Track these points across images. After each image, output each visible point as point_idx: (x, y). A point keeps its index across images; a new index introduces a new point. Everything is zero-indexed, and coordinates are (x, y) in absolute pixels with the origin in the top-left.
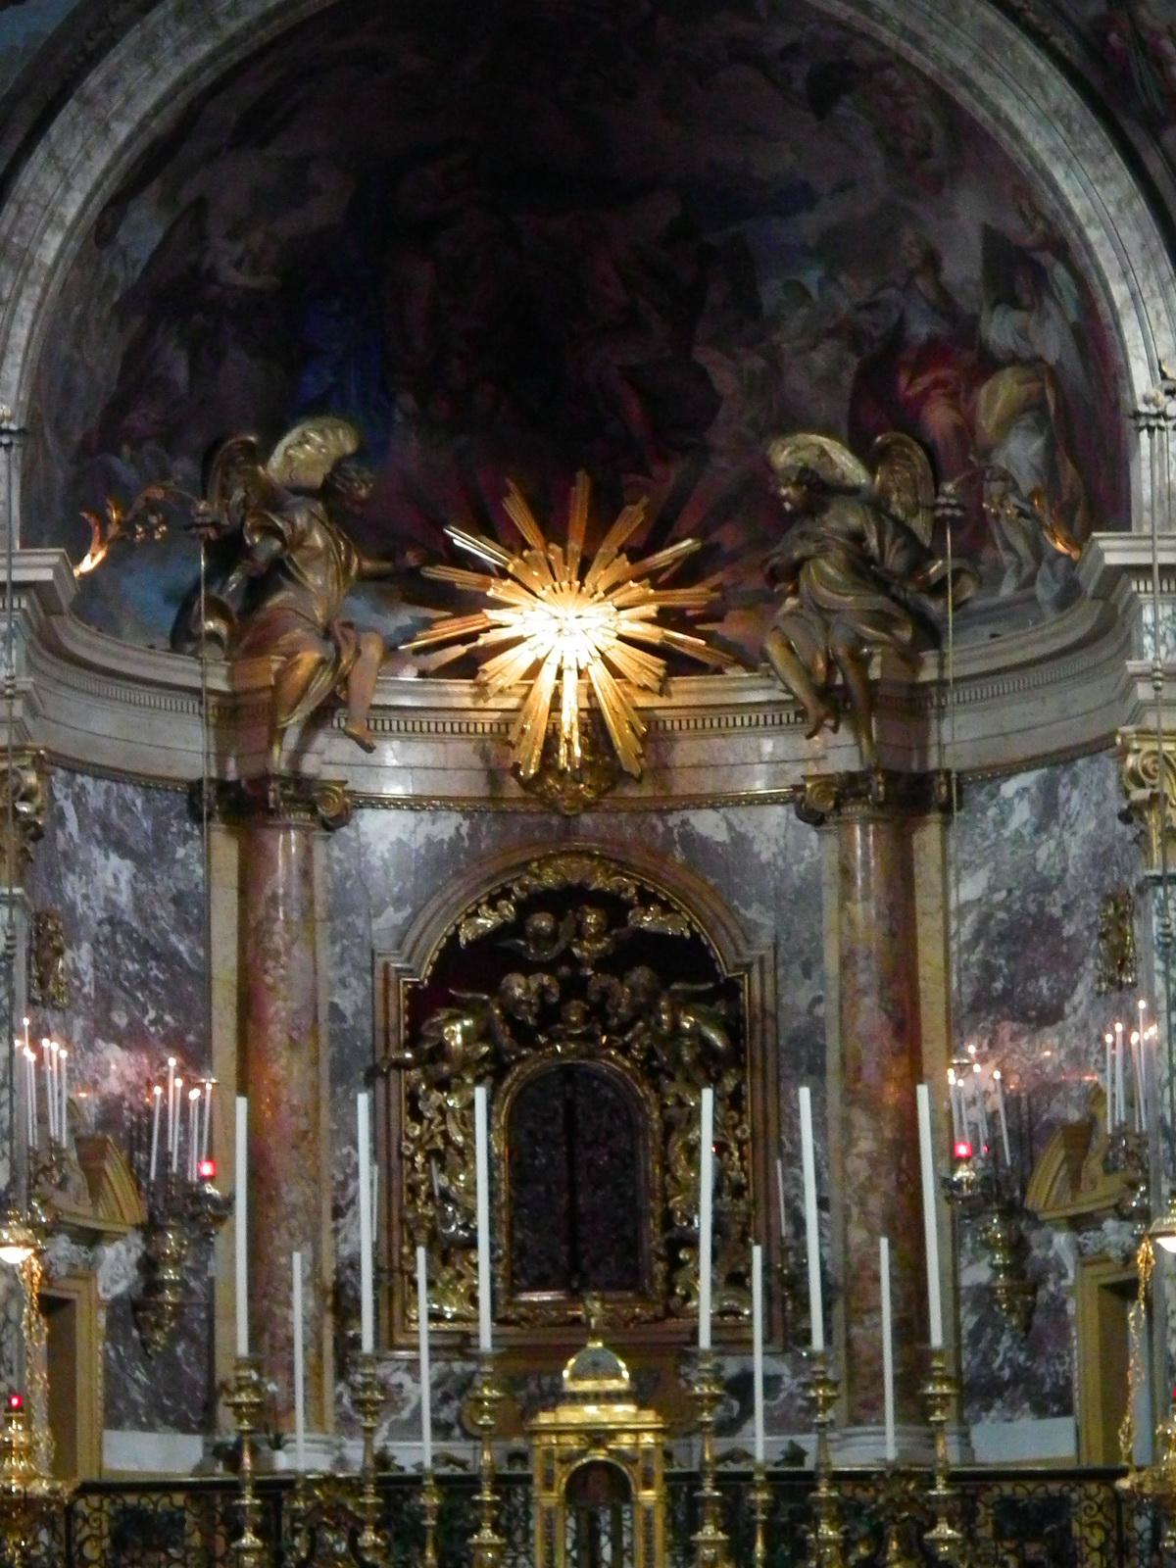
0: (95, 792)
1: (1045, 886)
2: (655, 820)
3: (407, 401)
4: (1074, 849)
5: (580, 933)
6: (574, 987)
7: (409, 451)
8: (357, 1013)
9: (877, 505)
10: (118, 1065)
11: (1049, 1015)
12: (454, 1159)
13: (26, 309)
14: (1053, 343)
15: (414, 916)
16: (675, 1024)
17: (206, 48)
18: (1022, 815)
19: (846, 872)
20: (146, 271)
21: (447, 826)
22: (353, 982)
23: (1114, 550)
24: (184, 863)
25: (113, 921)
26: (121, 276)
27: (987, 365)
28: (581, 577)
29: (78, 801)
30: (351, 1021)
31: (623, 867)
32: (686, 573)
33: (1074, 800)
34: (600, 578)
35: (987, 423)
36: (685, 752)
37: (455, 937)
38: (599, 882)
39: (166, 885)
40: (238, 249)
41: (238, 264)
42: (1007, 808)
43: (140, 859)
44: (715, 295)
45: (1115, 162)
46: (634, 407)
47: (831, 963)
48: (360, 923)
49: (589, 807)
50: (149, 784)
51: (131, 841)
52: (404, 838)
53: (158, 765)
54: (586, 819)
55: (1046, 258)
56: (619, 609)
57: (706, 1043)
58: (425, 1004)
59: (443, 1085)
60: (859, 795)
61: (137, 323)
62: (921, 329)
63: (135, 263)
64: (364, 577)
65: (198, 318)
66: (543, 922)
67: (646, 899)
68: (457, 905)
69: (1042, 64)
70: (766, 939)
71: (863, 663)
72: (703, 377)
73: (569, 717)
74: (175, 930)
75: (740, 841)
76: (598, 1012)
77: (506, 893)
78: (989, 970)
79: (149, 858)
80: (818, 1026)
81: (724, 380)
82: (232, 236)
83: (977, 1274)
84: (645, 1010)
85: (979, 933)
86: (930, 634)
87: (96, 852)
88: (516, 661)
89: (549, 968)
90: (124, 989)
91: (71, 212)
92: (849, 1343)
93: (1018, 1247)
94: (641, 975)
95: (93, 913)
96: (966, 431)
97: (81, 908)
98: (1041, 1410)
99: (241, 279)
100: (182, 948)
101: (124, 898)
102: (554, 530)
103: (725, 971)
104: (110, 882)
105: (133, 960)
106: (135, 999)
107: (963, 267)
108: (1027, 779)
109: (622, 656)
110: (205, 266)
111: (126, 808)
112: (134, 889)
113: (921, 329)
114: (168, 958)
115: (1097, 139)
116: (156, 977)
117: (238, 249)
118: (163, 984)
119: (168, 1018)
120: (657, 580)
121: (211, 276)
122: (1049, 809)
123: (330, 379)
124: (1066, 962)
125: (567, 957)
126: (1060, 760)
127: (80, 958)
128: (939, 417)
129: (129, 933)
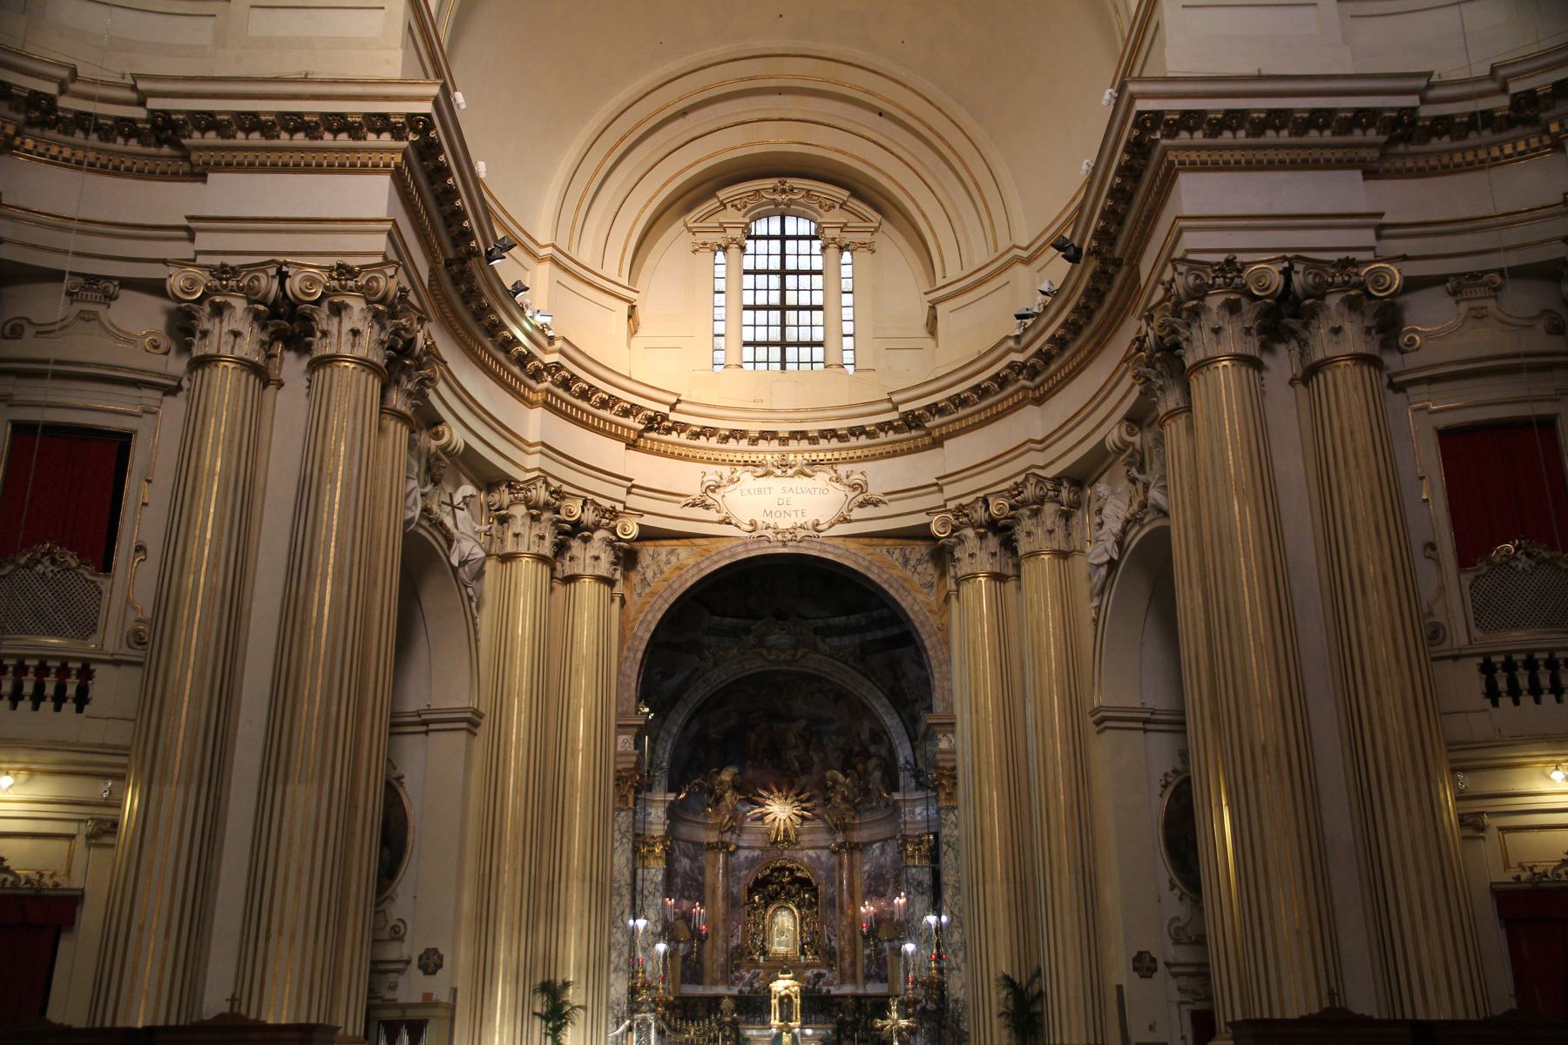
0: (682, 845)
1: (882, 867)
3: (750, 762)
4: (888, 859)
5: (784, 876)
6: (783, 888)
7: (750, 773)
9: (846, 786)
10: (685, 904)
11: (883, 895)
13: (670, 743)
14: (884, 752)
17: (708, 689)
18: (877, 852)
19: (841, 865)
21: (757, 853)
23: (897, 796)
25: (685, 872)
27: (870, 756)
29: (679, 846)
31: (794, 862)
32: (808, 800)
33: (888, 849)
34: (789, 801)
35: (870, 769)
36: (805, 838)
37: (757, 878)
38: (789, 865)
39: (697, 864)
42: (874, 850)
44: (814, 740)
45: (896, 715)
46: (797, 764)
47: (837, 883)
50: (694, 843)
55: (881, 734)
58: (751, 892)
59: (755, 909)
62: (857, 749)
64: (740, 799)
66: (776, 874)
67: (799, 869)
69: (881, 694)
72: (811, 758)
73: (782, 828)
75: (818, 857)
76: (788, 894)
78: (870, 885)
79: (694, 859)
80: (834, 897)
81: (815, 759)
83: (867, 952)
84: (798, 893)
85: (868, 877)
86: (858, 812)
88: (771, 817)
89: (777, 884)
91: (680, 722)
92: (841, 968)
93: (875, 945)
94: (797, 886)
95: (681, 871)
96: (866, 770)
98: (881, 982)
101: (688, 867)
102: (780, 791)
103: (814, 884)
107: (865, 736)
108: (878, 844)
109: (793, 817)
111: (689, 849)
113: (857, 749)
114: (697, 881)
115: (892, 710)
120: (801, 801)
122: (883, 851)
124: (887, 884)
125: (781, 881)
126: (885, 840)
127: (678, 881)
128: (860, 767)
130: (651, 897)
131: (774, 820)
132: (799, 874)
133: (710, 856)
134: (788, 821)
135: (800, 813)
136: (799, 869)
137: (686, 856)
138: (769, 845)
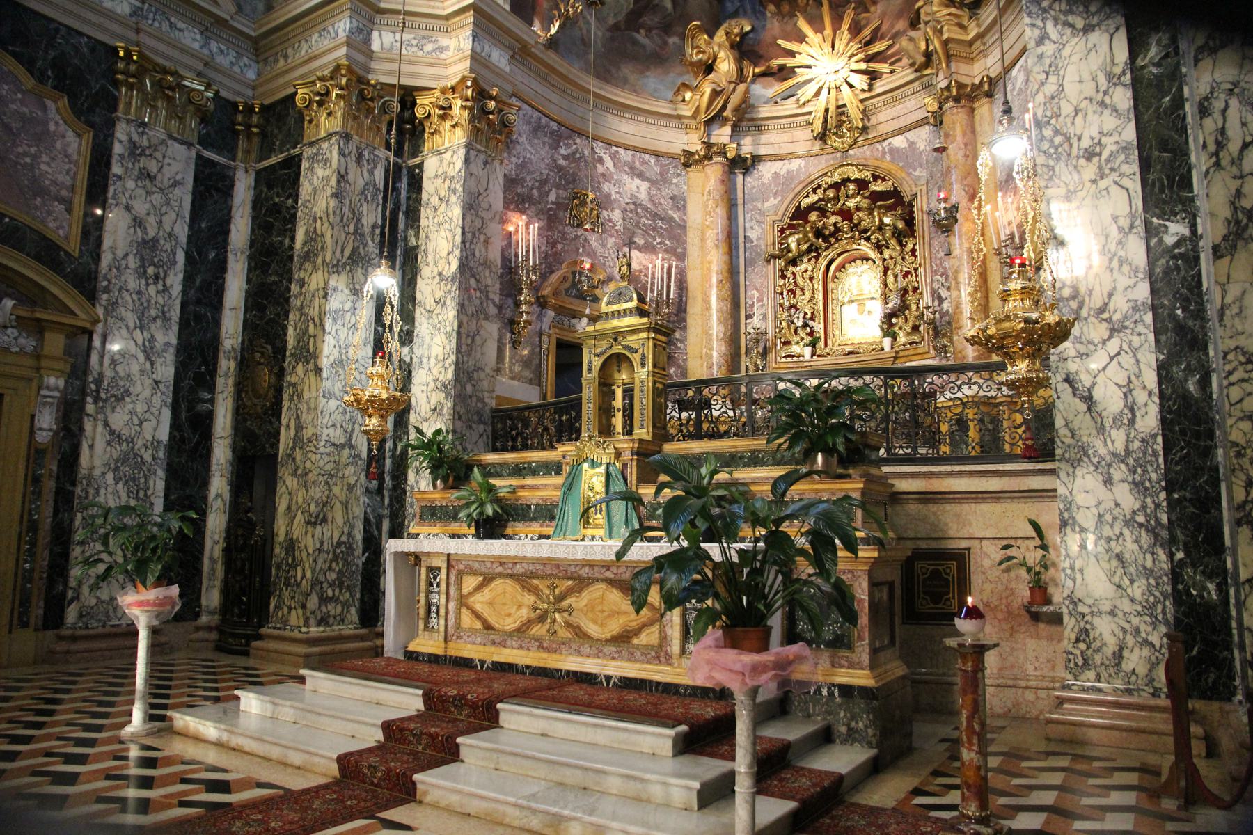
0: (625, 156)
2: (878, 145)
3: (772, 7)
8: (759, 239)
12: (798, 292)
15: (782, 201)
16: (881, 220)
28: (833, 47)
29: (613, 156)
34: (840, 46)
38: (854, 174)
43: (653, 182)
48: (759, 205)
49: (851, 147)
50: (657, 154)
51: (647, 175)
53: (663, 148)
54: (851, 152)
56: (850, 57)
57: (895, 227)
59: (794, 262)
60: (947, 99)
67: (876, 178)
68: (799, 192)
70: (923, 181)
71: (941, 31)
77: (819, 187)
87: (625, 177)
97: (613, 197)
102: (819, 29)
104: (635, 189)
111: (644, 162)
129: (646, 209)
130: (443, 208)
131: (817, 94)
132: (878, 187)
133: (694, 174)
134: (845, 88)
135: (863, 66)
136: (876, 178)
137: (641, 176)
138: (818, 144)
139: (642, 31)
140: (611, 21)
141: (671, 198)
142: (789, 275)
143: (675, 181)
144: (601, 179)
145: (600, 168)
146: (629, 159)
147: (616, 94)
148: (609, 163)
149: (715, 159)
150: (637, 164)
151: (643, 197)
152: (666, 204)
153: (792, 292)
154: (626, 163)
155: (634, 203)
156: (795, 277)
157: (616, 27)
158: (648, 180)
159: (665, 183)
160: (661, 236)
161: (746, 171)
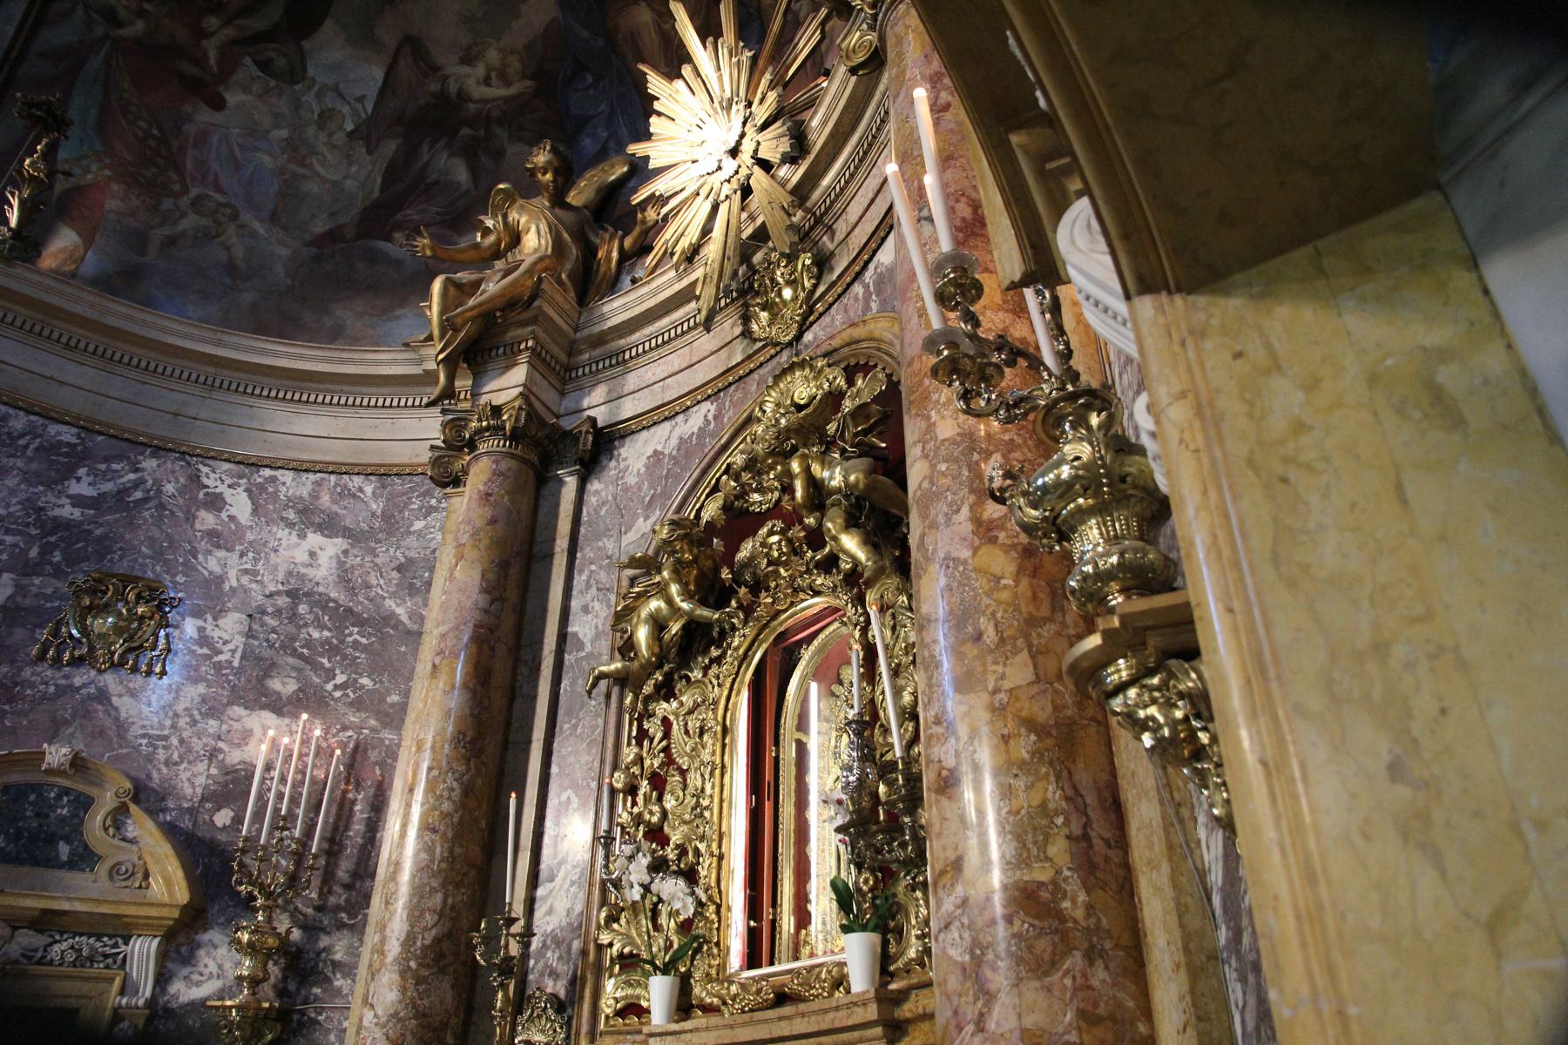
20: (377, 104)
22: (596, 605)
24: (420, 534)
26: (346, 110)
30: (588, 648)
40: (481, 70)
41: (487, 81)
51: (348, 522)
52: (659, 448)
61: (390, 147)
63: (361, 99)
65: (465, 131)
74: (393, 595)
82: (468, 59)
87: (282, 532)
90: (301, 657)
99: (497, 91)
100: (400, 611)
104: (305, 558)
105: (322, 627)
106: (317, 667)
110: (453, 88)
112: (341, 564)
116: (356, 642)
117: (481, 70)
118: (365, 649)
119: (365, 681)
121: (463, 97)
123: (605, 134)
129: (322, 603)
137: (329, 526)
139: (398, 236)
140: (320, 226)
141: (399, 569)
142: (654, 727)
143: (419, 525)
144: (203, 545)
145: (206, 520)
146: (305, 492)
147: (262, 352)
148: (239, 505)
149: (482, 448)
150: (325, 500)
151: (323, 572)
152: (382, 584)
153: (658, 783)
154: (291, 502)
155: (288, 593)
156: (667, 735)
157: (333, 236)
158: (347, 533)
159: (390, 534)
160: (352, 666)
161: (589, 466)
